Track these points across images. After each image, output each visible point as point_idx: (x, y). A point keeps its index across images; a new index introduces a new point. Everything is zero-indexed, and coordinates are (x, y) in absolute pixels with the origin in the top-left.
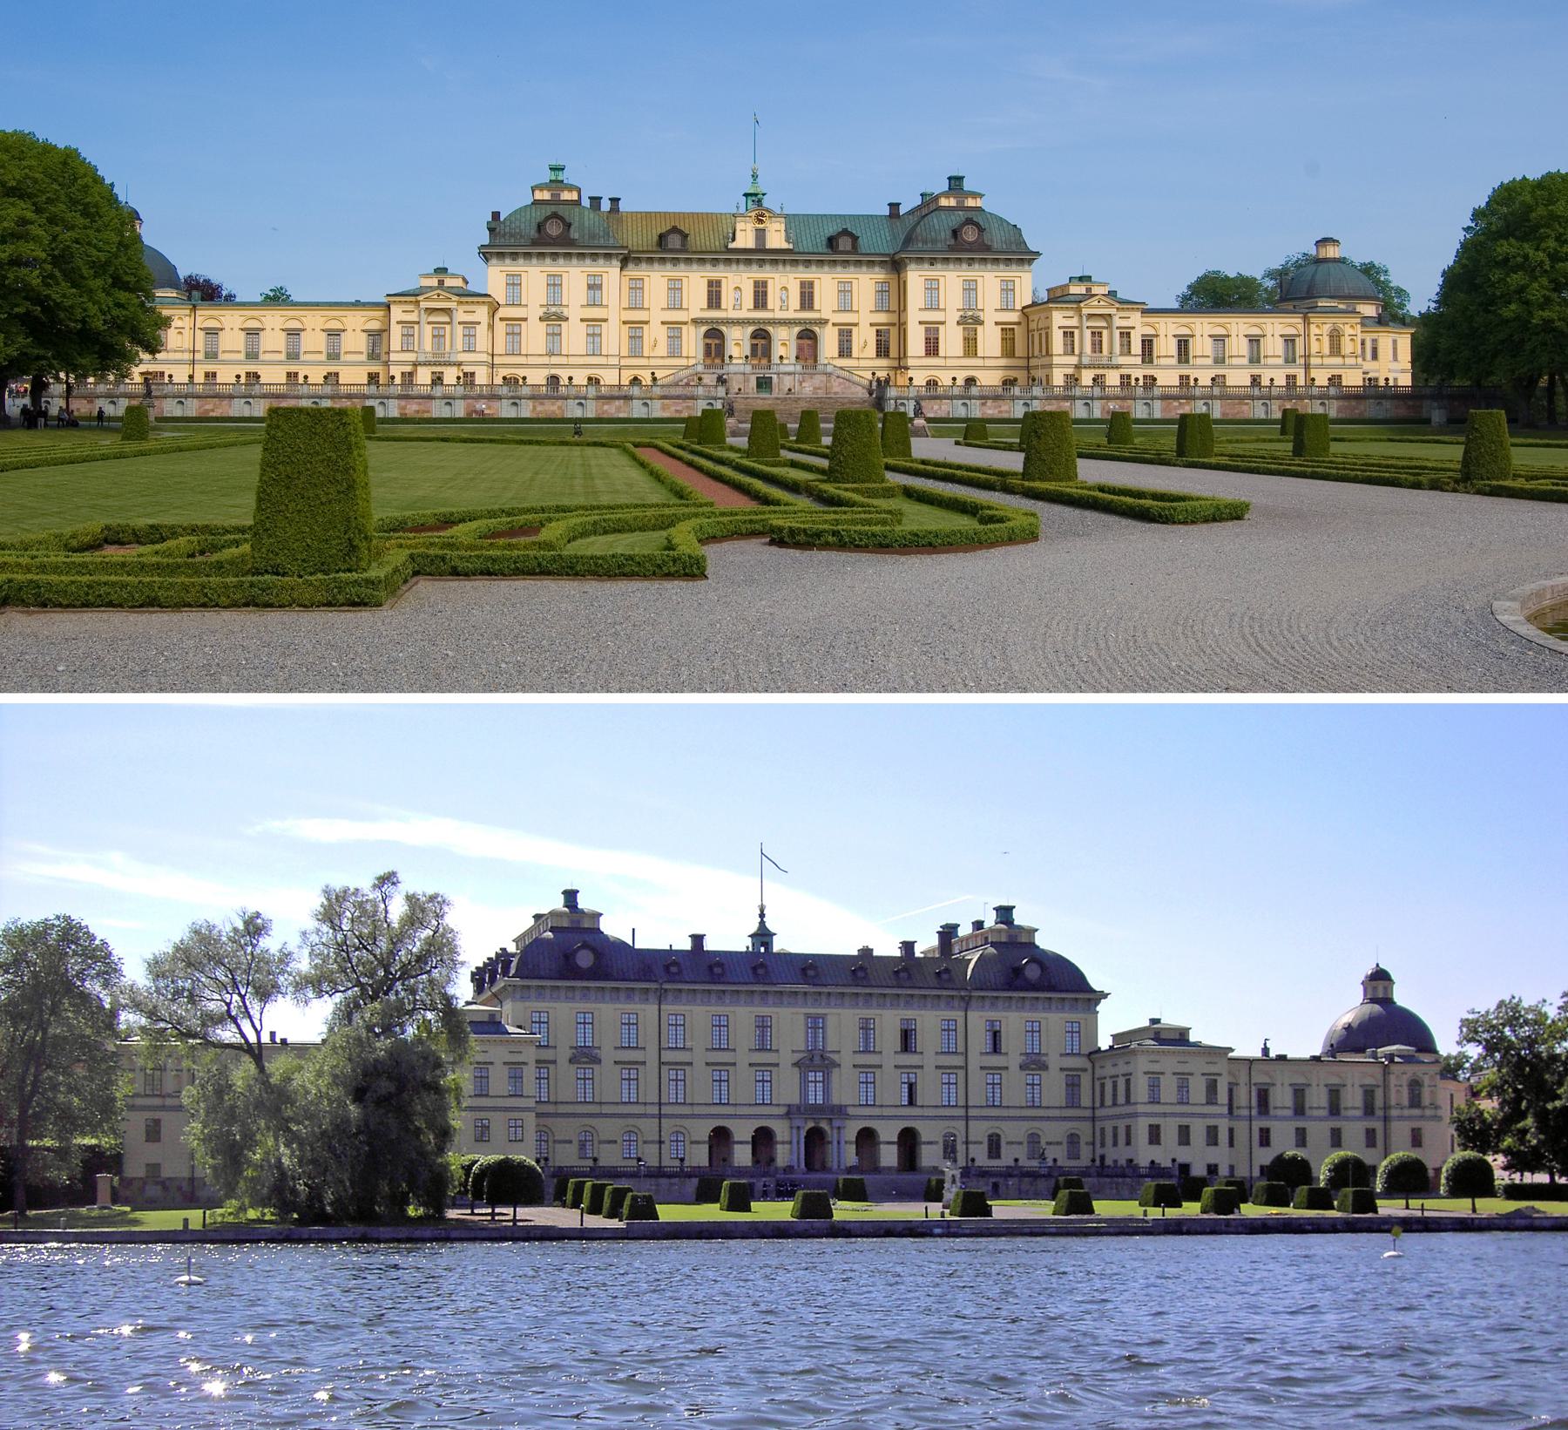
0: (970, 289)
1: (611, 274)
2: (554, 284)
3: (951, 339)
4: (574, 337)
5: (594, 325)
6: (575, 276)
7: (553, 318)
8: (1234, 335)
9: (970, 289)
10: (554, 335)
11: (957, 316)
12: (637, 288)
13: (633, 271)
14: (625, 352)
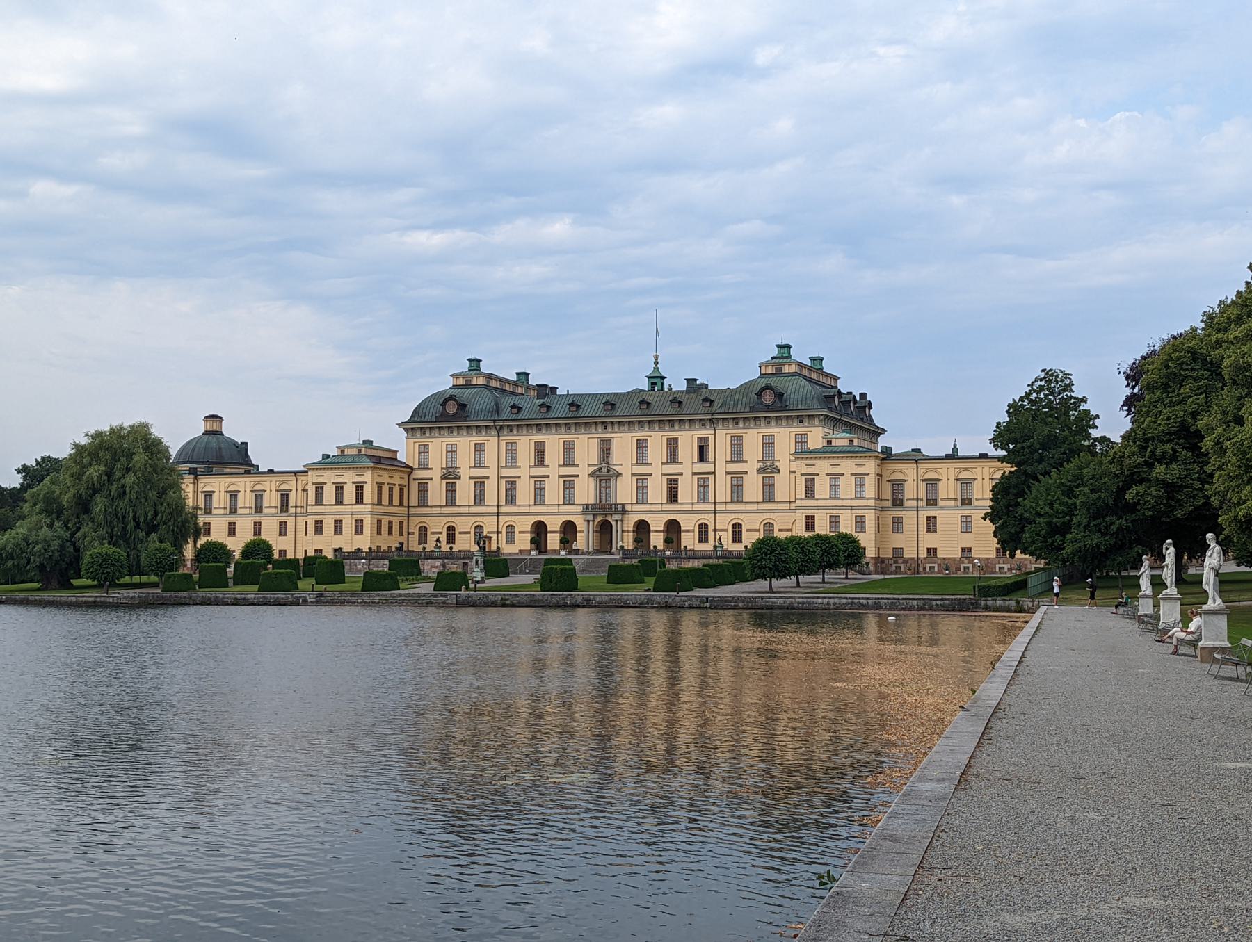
0: (768, 443)
1: (490, 442)
2: (451, 451)
3: (752, 487)
4: (465, 491)
5: (480, 484)
6: (465, 444)
7: (450, 476)
8: (945, 479)
9: (768, 443)
10: (451, 491)
11: (756, 466)
12: (511, 448)
13: (506, 438)
14: (503, 502)
